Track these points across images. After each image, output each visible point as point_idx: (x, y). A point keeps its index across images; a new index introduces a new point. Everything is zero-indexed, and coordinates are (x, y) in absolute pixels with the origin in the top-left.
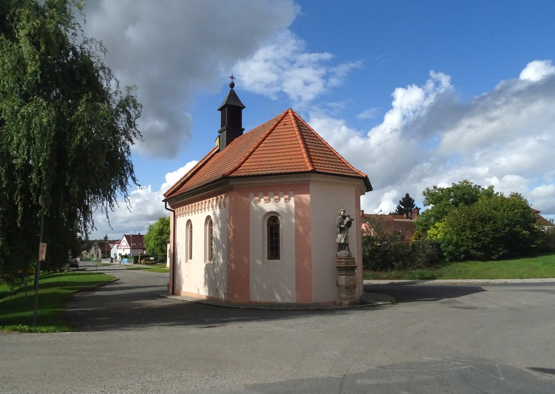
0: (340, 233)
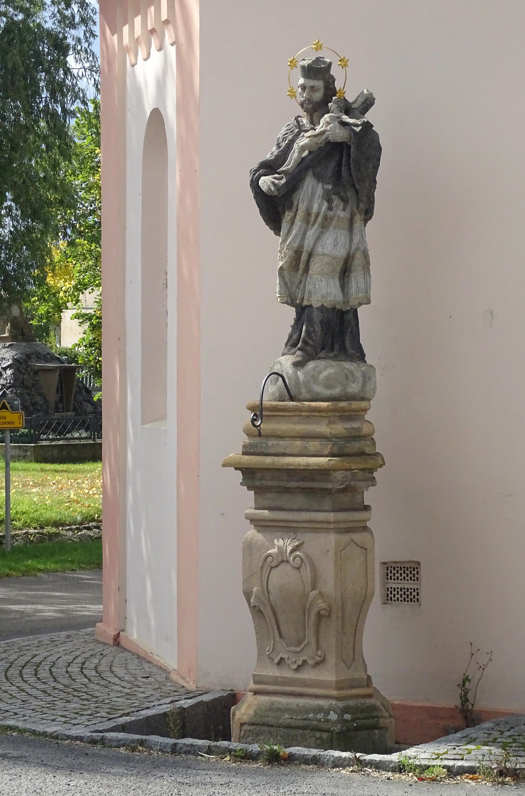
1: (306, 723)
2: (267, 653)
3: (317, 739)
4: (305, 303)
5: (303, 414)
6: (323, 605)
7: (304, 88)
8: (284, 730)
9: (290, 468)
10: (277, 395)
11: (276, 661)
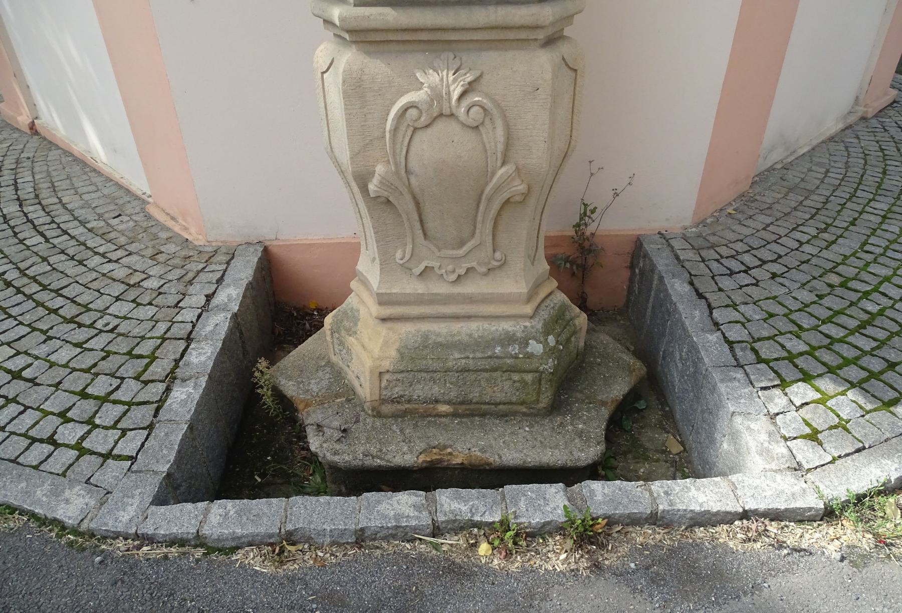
1: (494, 363)
2: (401, 262)
3: (514, 382)
6: (522, 188)
8: (456, 375)
11: (417, 271)
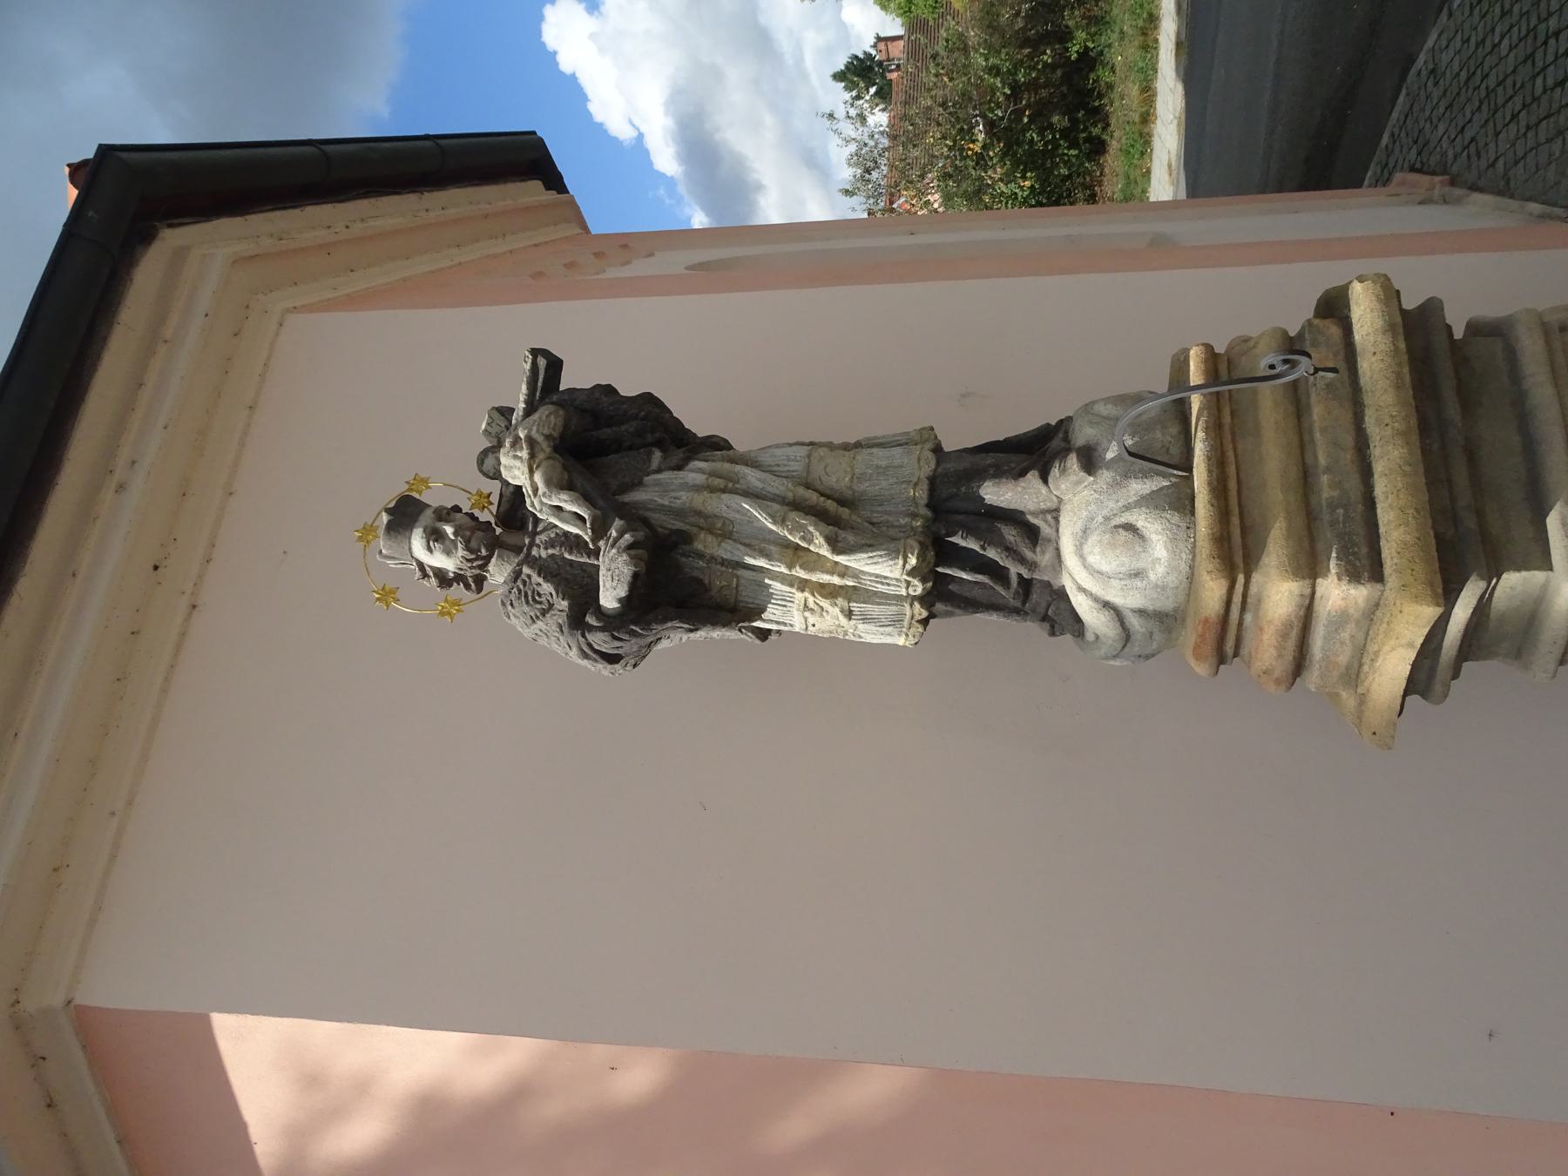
0: (732, 607)
4: (922, 494)
5: (1227, 419)
7: (434, 536)
9: (1407, 378)
10: (1176, 518)
